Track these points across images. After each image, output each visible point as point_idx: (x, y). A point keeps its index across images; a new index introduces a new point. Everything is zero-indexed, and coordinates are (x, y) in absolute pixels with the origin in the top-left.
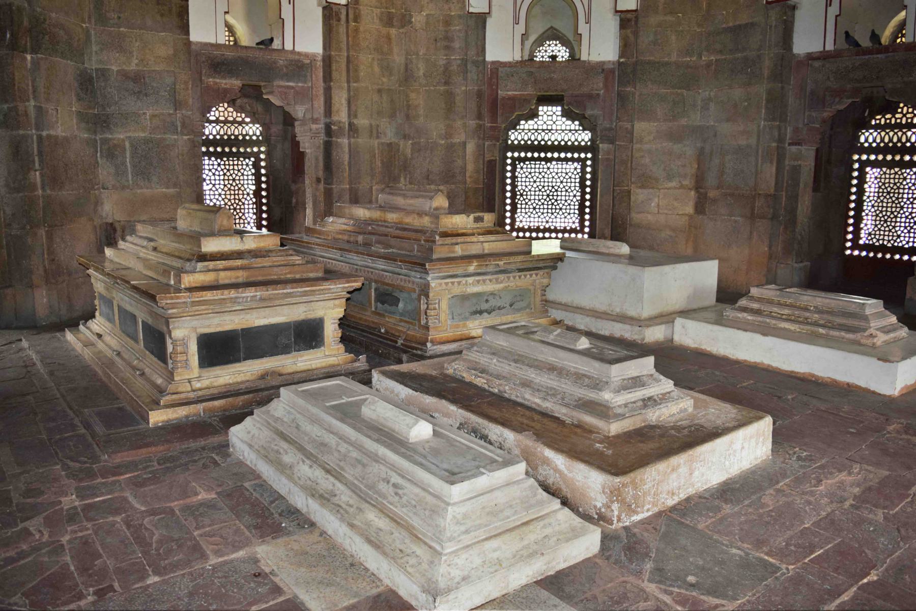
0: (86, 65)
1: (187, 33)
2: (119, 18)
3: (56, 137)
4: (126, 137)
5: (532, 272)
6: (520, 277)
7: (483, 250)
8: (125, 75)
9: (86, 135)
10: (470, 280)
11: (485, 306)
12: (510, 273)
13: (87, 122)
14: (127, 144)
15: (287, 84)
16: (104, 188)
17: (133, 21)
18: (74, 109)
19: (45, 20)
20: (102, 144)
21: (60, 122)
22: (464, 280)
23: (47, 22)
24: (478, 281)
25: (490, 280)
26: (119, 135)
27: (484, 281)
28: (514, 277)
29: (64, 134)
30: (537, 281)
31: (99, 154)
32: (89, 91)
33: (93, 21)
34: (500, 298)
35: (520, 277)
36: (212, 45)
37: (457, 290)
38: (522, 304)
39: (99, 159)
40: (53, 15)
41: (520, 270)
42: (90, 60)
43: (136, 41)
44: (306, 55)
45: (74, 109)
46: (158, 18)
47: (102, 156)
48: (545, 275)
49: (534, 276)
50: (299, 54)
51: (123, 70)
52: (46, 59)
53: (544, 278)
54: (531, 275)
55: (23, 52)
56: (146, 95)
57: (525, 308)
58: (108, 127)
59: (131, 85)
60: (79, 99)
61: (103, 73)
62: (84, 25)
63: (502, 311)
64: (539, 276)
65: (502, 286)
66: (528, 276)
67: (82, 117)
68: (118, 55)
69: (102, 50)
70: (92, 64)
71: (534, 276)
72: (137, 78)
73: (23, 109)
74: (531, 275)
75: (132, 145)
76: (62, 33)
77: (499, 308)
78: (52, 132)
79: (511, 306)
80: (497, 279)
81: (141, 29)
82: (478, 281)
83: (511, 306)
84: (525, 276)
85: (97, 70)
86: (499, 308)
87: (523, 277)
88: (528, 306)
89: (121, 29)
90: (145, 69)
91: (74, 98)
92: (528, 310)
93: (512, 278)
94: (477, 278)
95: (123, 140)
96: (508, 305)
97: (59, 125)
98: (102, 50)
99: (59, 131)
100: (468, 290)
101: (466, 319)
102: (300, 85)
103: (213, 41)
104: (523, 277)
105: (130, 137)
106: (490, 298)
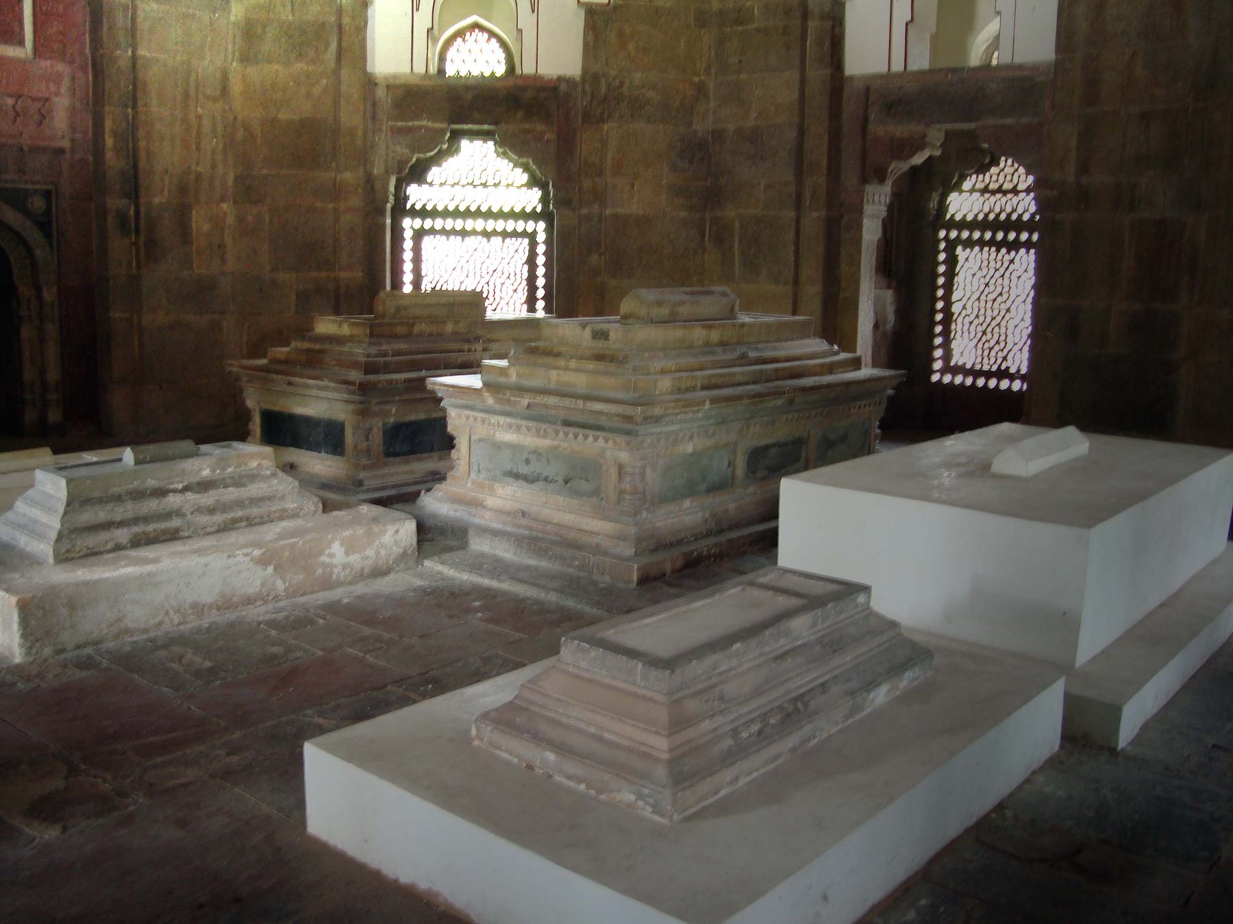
2: (740, 61)
5: (598, 433)
6: (576, 436)
7: (549, 380)
9: (683, 214)
10: (502, 420)
11: (524, 470)
12: (550, 422)
14: (737, 224)
15: (1001, 122)
18: (664, 182)
19: (622, 84)
22: (494, 419)
23: (627, 84)
24: (510, 426)
25: (529, 429)
26: (730, 212)
27: (519, 427)
28: (566, 434)
30: (608, 453)
31: (707, 237)
34: (549, 462)
35: (576, 436)
37: (481, 431)
38: (584, 486)
40: (639, 75)
41: (567, 423)
43: (756, 88)
44: (1035, 68)
45: (664, 182)
48: (623, 445)
49: (601, 440)
50: (1020, 67)
53: (619, 450)
54: (596, 439)
57: (591, 494)
61: (719, 135)
62: (696, 79)
63: (551, 486)
64: (610, 444)
65: (545, 443)
66: (591, 439)
70: (700, 127)
71: (601, 440)
72: (753, 136)
74: (596, 439)
75: (742, 227)
76: (651, 94)
77: (546, 479)
78: (619, 210)
79: (566, 482)
80: (538, 431)
82: (510, 426)
83: (566, 482)
84: (586, 437)
86: (546, 479)
87: (580, 437)
88: (596, 492)
92: (595, 499)
93: (561, 434)
94: (508, 420)
96: (560, 479)
99: (634, 208)
100: (497, 435)
101: (494, 479)
102: (1024, 120)
103: (883, 69)
104: (580, 437)
106: (533, 458)
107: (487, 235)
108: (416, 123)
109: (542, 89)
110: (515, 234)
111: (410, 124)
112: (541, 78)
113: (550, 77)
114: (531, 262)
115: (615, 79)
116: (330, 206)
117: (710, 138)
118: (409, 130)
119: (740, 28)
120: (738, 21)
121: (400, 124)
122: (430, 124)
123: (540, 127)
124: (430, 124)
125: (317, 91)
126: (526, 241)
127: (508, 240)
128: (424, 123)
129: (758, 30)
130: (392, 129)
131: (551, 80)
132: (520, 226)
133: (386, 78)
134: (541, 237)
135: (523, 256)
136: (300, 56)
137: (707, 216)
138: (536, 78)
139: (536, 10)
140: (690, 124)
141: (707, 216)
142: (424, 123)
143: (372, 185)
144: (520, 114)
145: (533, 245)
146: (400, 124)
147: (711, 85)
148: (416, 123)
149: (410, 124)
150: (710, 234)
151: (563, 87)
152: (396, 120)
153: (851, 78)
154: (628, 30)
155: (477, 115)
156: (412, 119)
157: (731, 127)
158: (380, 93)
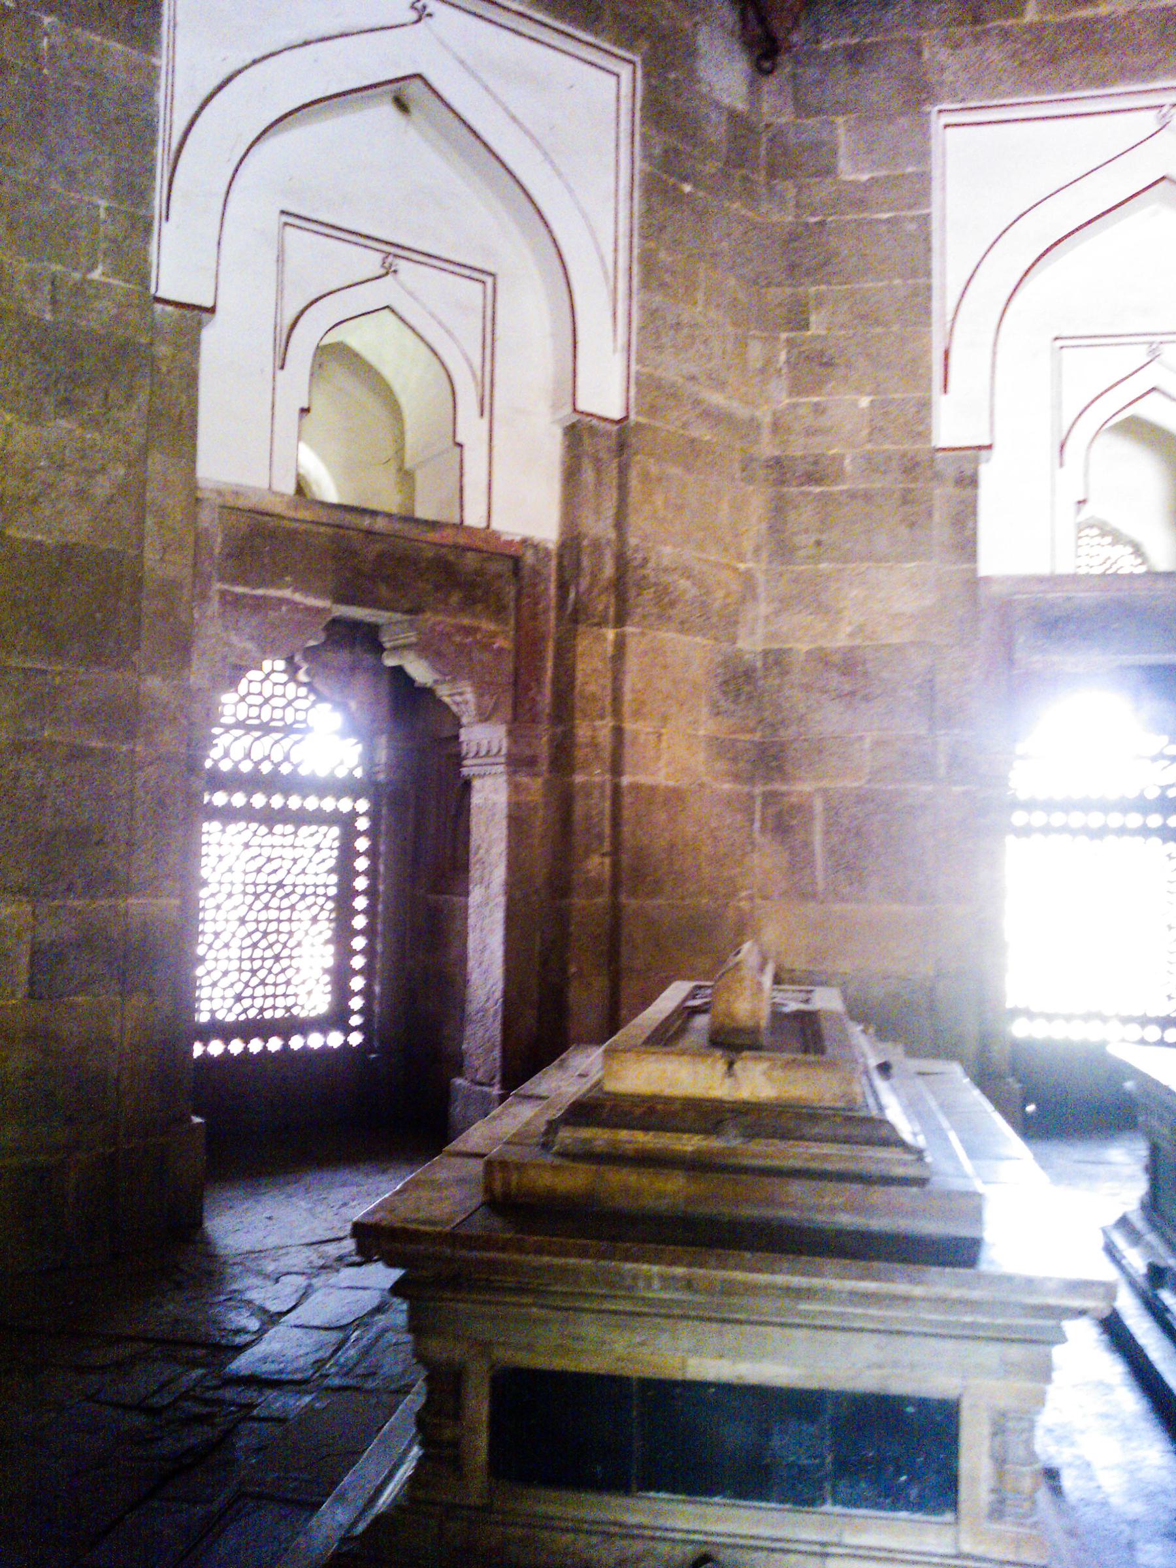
0: (740, 644)
1: (973, 557)
2: (819, 543)
3: (653, 789)
4: (818, 790)
8: (822, 659)
13: (735, 760)
16: (765, 898)
17: (848, 546)
19: (645, 560)
20: (765, 805)
21: (666, 757)
29: (671, 783)
31: (757, 825)
32: (743, 698)
33: (765, 555)
36: (1041, 580)
39: (756, 835)
40: (668, 550)
42: (752, 633)
45: (702, 732)
46: (903, 531)
47: (763, 830)
51: (822, 649)
52: (643, 634)
55: (599, 625)
56: (866, 699)
58: (780, 769)
59: (835, 680)
60: (717, 713)
61: (777, 660)
67: (721, 748)
68: (809, 618)
69: (777, 613)
73: (589, 733)
76: (684, 583)
78: (644, 779)
81: (862, 559)
85: (766, 653)
89: (823, 566)
90: (868, 643)
91: (705, 711)
95: (810, 795)
97: (662, 763)
98: (777, 613)
99: (661, 776)
105: (825, 791)
107: (269, 818)
108: (273, 592)
109: (493, 556)
110: (320, 818)
111: (260, 592)
112: (496, 535)
113: (510, 538)
114: (344, 869)
115: (636, 550)
116: (124, 748)
117: (759, 664)
118: (260, 605)
119: (818, 490)
120: (812, 478)
121: (240, 590)
122: (298, 597)
123: (488, 626)
124: (298, 597)
125: (102, 488)
126: (335, 831)
127: (305, 830)
128: (287, 593)
129: (853, 495)
130: (223, 594)
131: (510, 543)
132: (329, 804)
133: (220, 493)
134: (363, 824)
135: (330, 857)
136: (68, 405)
137: (758, 790)
138: (488, 533)
139: (487, 413)
140: (733, 641)
141: (758, 790)
142: (287, 593)
143: (209, 709)
144: (455, 599)
145: (349, 834)
146: (240, 590)
147: (761, 578)
148: (273, 592)
149: (260, 592)
150: (764, 820)
151: (529, 558)
152: (235, 581)
153: (988, 580)
154: (654, 470)
155: (383, 590)
156: (264, 584)
157: (803, 647)
158: (207, 518)
